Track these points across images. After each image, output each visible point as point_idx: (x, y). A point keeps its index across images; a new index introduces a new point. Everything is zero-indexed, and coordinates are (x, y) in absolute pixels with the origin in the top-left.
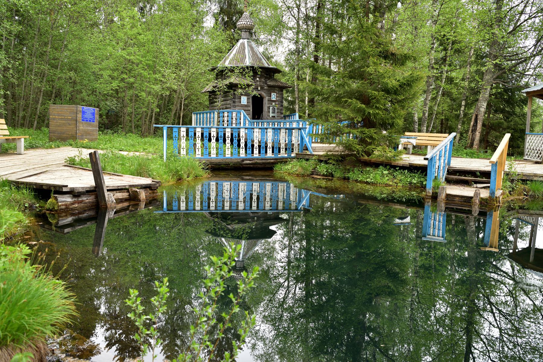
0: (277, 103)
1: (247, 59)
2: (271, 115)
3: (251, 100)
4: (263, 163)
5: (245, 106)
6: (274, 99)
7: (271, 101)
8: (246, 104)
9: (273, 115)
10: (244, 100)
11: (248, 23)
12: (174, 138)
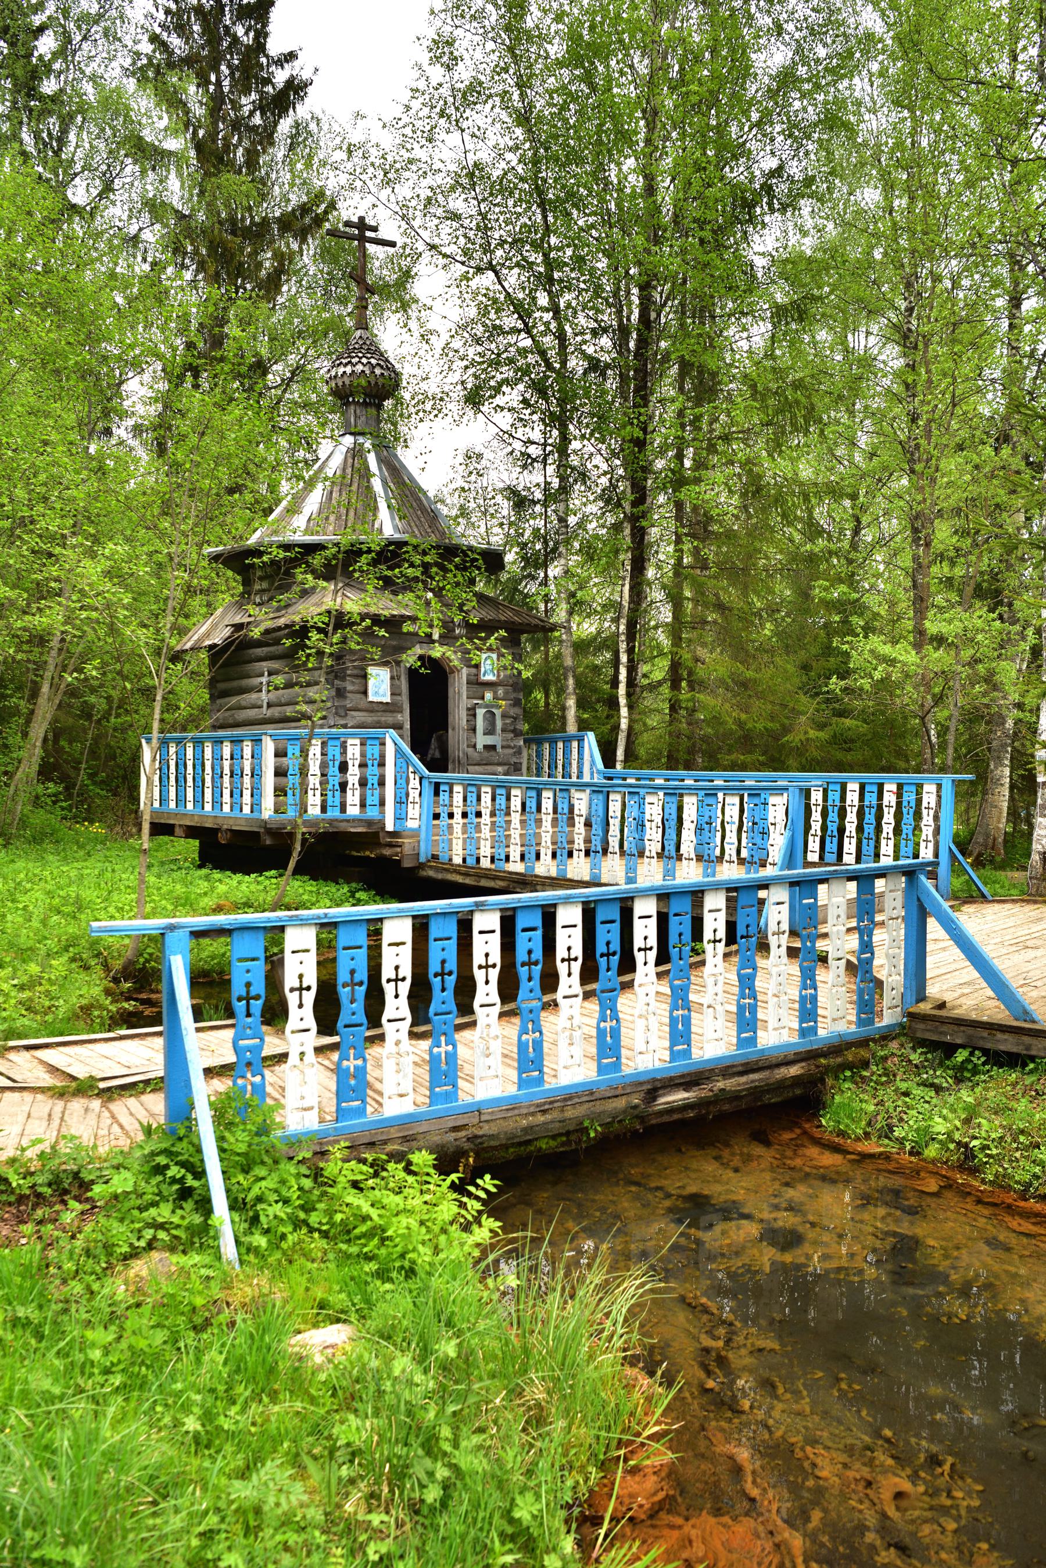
0: (501, 692)
1: (384, 513)
2: (482, 740)
3: (404, 685)
4: (756, 1092)
5: (385, 708)
6: (490, 678)
7: (477, 685)
8: (387, 699)
9: (489, 740)
10: (380, 684)
11: (378, 371)
12: (240, 1007)
